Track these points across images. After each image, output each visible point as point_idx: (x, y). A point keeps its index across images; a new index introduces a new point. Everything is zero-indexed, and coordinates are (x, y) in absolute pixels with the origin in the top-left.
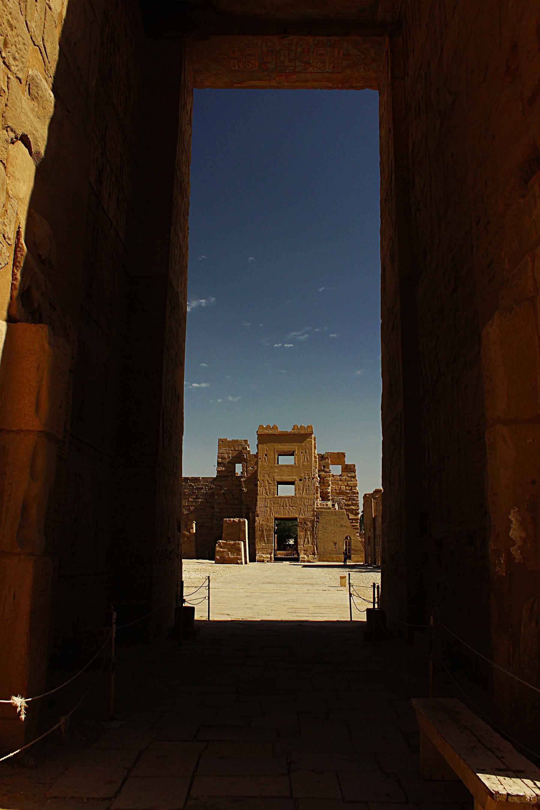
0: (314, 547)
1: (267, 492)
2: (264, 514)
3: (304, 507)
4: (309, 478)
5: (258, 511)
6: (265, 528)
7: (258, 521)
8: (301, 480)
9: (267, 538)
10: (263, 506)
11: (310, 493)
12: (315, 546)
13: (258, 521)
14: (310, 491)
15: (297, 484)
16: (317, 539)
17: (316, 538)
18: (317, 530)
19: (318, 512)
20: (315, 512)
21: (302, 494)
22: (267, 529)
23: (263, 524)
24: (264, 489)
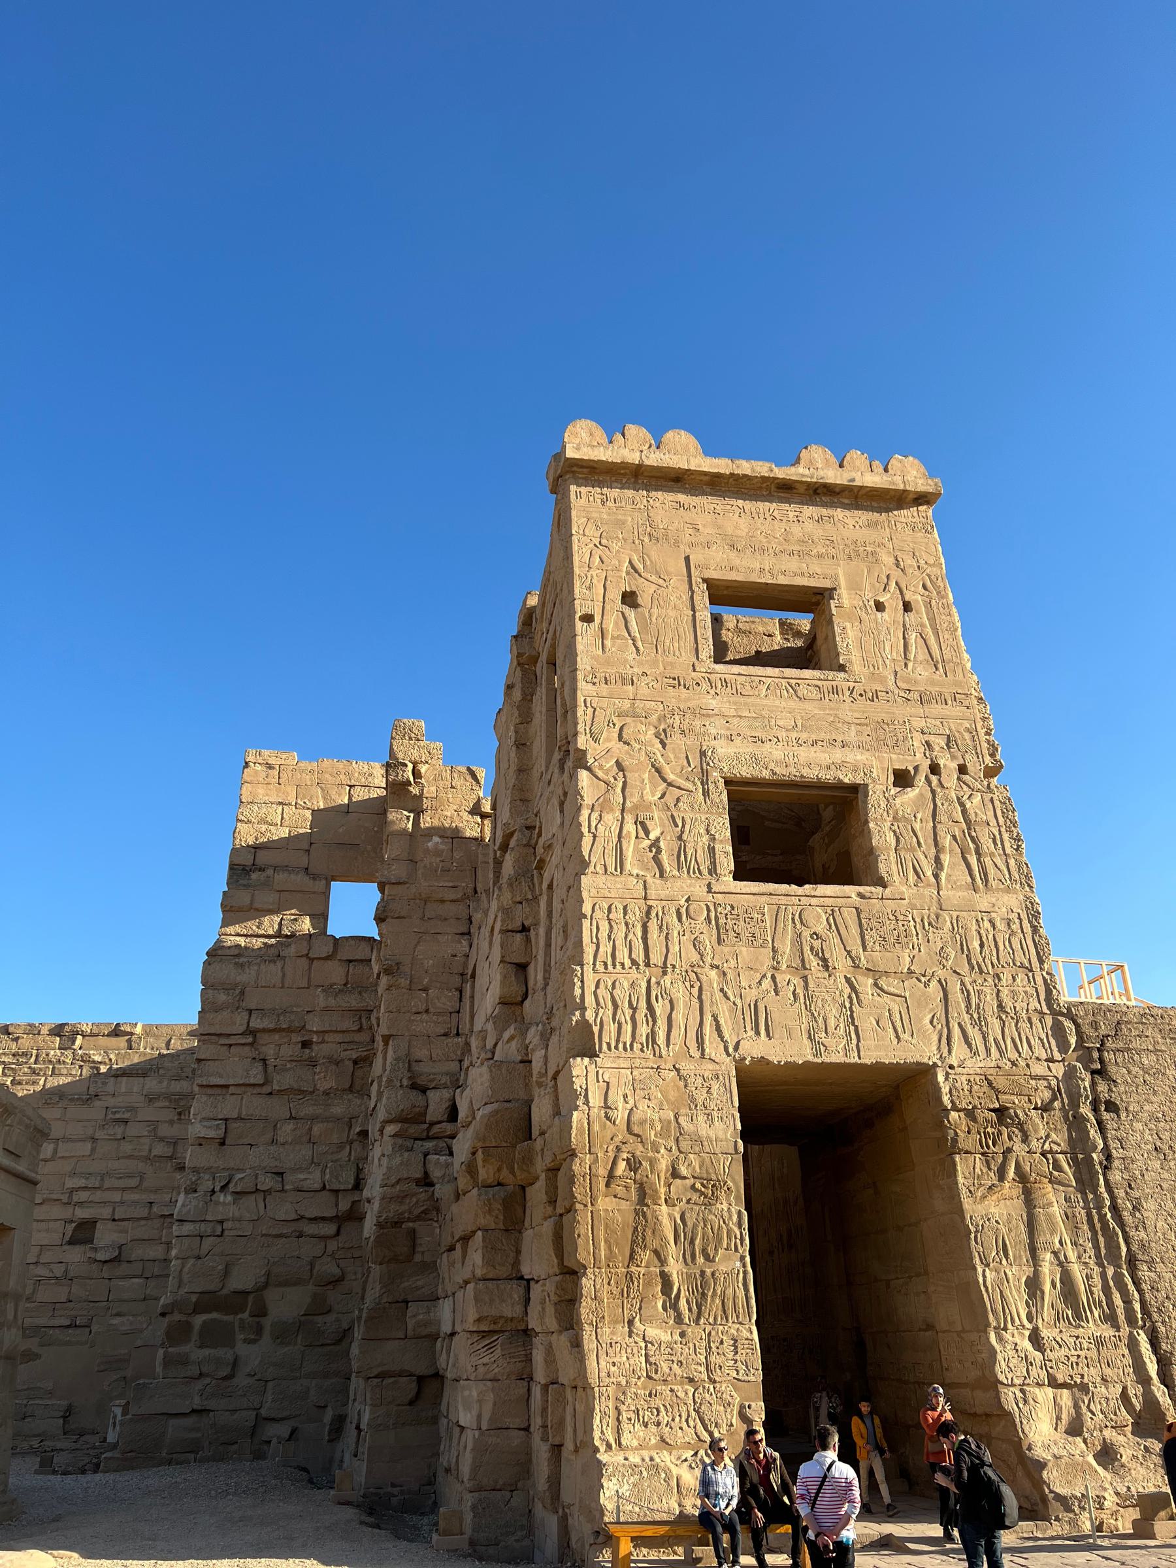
0: (1133, 1345)
1: (655, 844)
2: (644, 1030)
3: (967, 980)
4: (962, 769)
5: (590, 1000)
6: (663, 1164)
7: (596, 1099)
8: (903, 779)
9: (689, 1258)
10: (634, 963)
11: (992, 872)
12: (1143, 1339)
13: (596, 1099)
14: (987, 860)
15: (883, 803)
16: (1144, 1272)
17: (1132, 1262)
18: (1116, 1176)
19: (1095, 1025)
20: (1068, 1024)
21: (936, 876)
22: (683, 1170)
23: (642, 1122)
24: (630, 827)
